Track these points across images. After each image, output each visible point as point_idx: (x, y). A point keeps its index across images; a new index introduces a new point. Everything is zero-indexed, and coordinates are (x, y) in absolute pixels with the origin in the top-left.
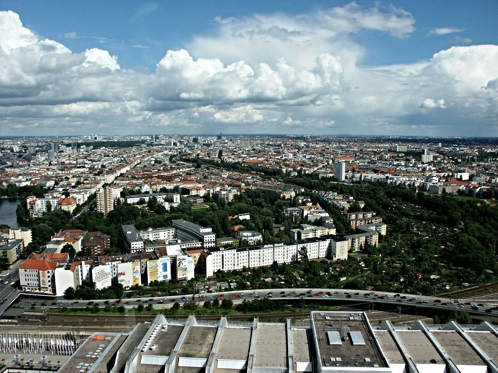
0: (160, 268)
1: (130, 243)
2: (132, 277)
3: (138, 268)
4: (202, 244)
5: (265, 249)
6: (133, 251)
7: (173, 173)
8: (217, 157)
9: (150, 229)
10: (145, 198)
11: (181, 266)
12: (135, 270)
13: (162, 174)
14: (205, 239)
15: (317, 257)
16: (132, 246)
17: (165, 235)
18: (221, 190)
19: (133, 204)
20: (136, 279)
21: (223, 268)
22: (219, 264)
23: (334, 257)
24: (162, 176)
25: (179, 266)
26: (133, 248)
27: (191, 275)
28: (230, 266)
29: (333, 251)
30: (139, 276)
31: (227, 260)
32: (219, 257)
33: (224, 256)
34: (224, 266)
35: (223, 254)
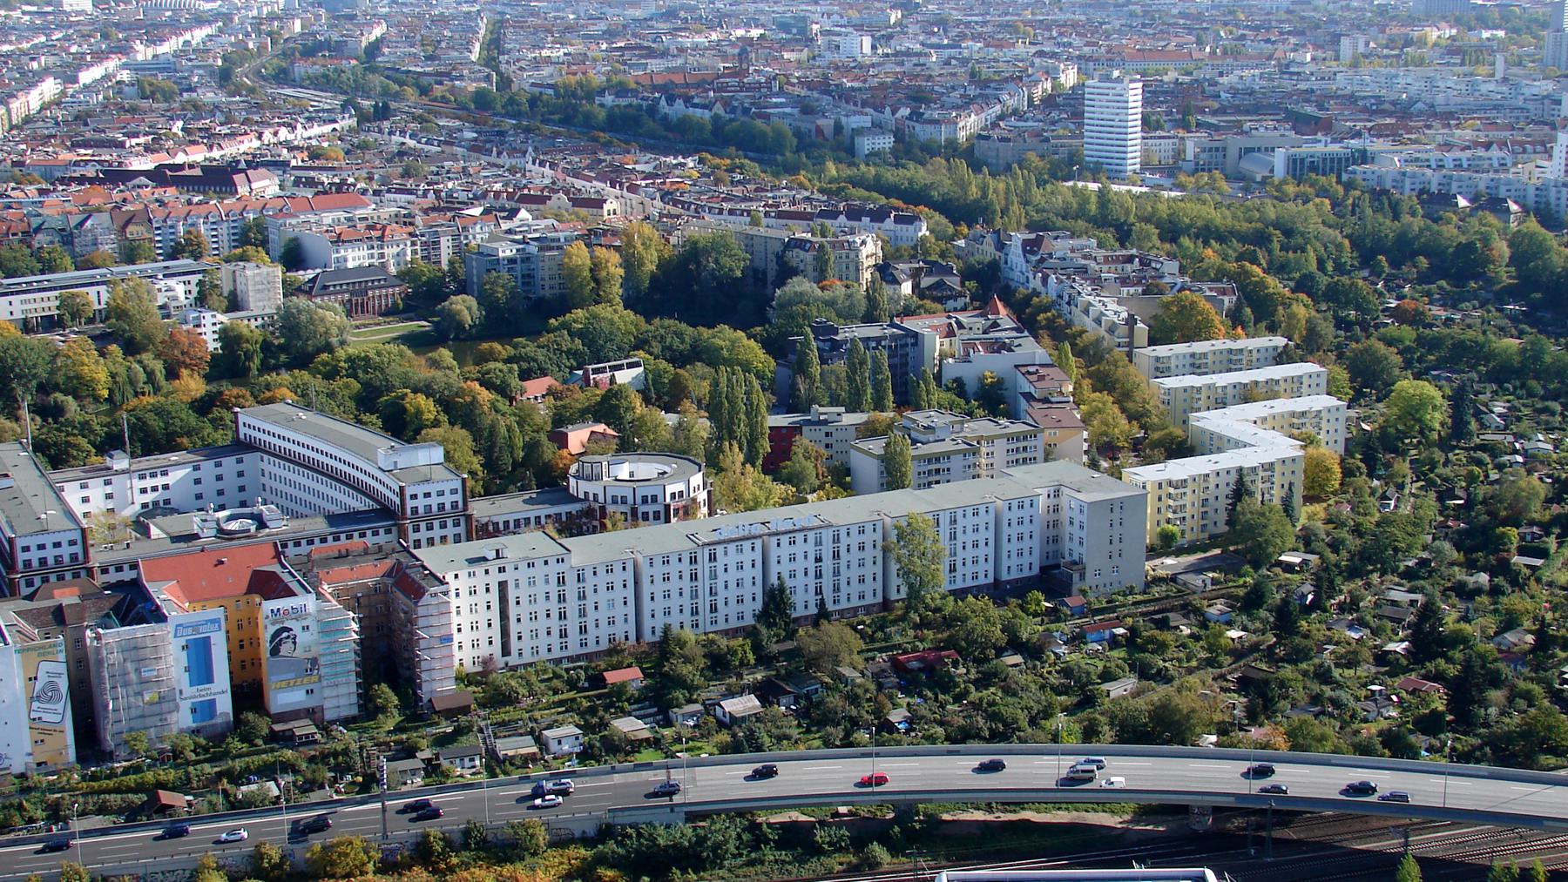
0: (173, 663)
1: (11, 541)
2: (26, 723)
3: (55, 671)
4: (402, 533)
5: (720, 550)
6: (30, 584)
7: (243, 148)
8: (474, 57)
9: (120, 462)
10: (92, 291)
11: (285, 649)
12: (39, 685)
13: (180, 159)
14: (410, 504)
15: (991, 579)
16: (21, 557)
17: (198, 489)
18: (493, 238)
19: (26, 326)
20: (44, 731)
21: (506, 651)
22: (483, 634)
23: (1076, 577)
24: (181, 167)
25: (275, 651)
26: (28, 564)
27: (340, 697)
28: (543, 641)
29: (1068, 545)
30: (60, 714)
31: (524, 610)
32: (482, 597)
33: (511, 586)
34: (514, 645)
35: (502, 577)
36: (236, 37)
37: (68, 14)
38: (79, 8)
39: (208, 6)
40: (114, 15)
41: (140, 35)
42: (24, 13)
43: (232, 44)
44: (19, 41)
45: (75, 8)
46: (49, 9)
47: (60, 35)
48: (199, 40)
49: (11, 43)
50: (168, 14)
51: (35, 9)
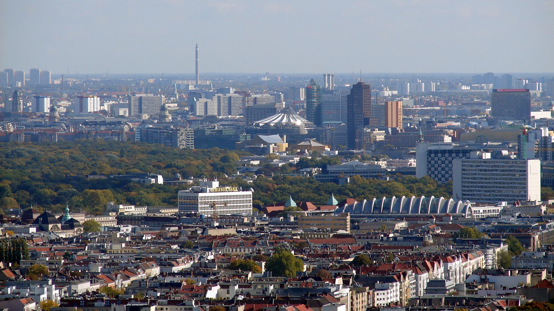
36: (536, 274)
37: (207, 223)
38: (228, 211)
39: (481, 211)
40: (294, 226)
41: (344, 267)
42: (122, 219)
43: (526, 290)
44: (110, 274)
45: (220, 210)
46: (169, 212)
47: (188, 265)
48: (459, 278)
49: (93, 278)
50: (401, 225)
51: (142, 211)
